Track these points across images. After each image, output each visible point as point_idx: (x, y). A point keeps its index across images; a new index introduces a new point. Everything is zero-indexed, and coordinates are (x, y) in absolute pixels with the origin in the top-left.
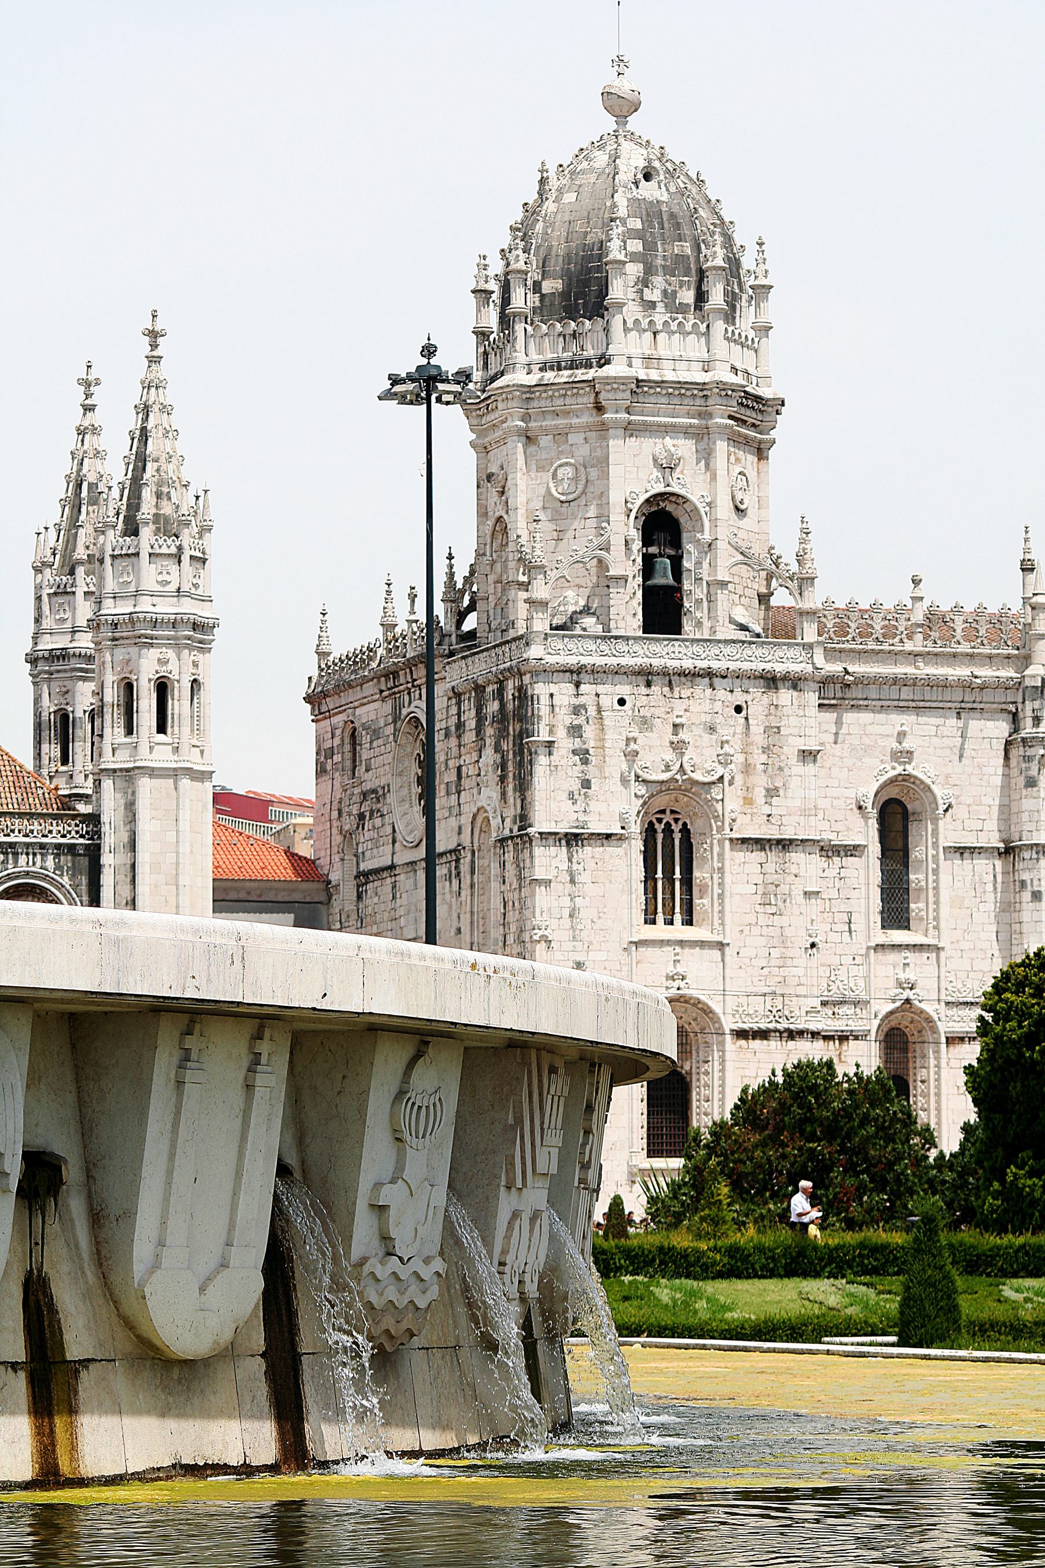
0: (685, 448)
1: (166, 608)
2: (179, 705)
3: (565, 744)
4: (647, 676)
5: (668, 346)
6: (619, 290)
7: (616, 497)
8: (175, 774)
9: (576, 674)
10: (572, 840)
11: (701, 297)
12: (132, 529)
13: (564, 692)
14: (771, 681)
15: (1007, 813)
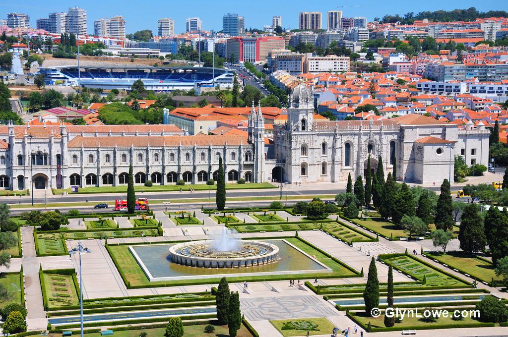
0: (305, 114)
1: (261, 128)
2: (262, 136)
3: (294, 141)
4: (302, 135)
5: (304, 106)
6: (300, 101)
7: (299, 119)
8: (261, 142)
9: (296, 135)
10: (295, 149)
11: (307, 100)
12: (257, 120)
13: (294, 137)
14: (313, 135)
15: (333, 145)
